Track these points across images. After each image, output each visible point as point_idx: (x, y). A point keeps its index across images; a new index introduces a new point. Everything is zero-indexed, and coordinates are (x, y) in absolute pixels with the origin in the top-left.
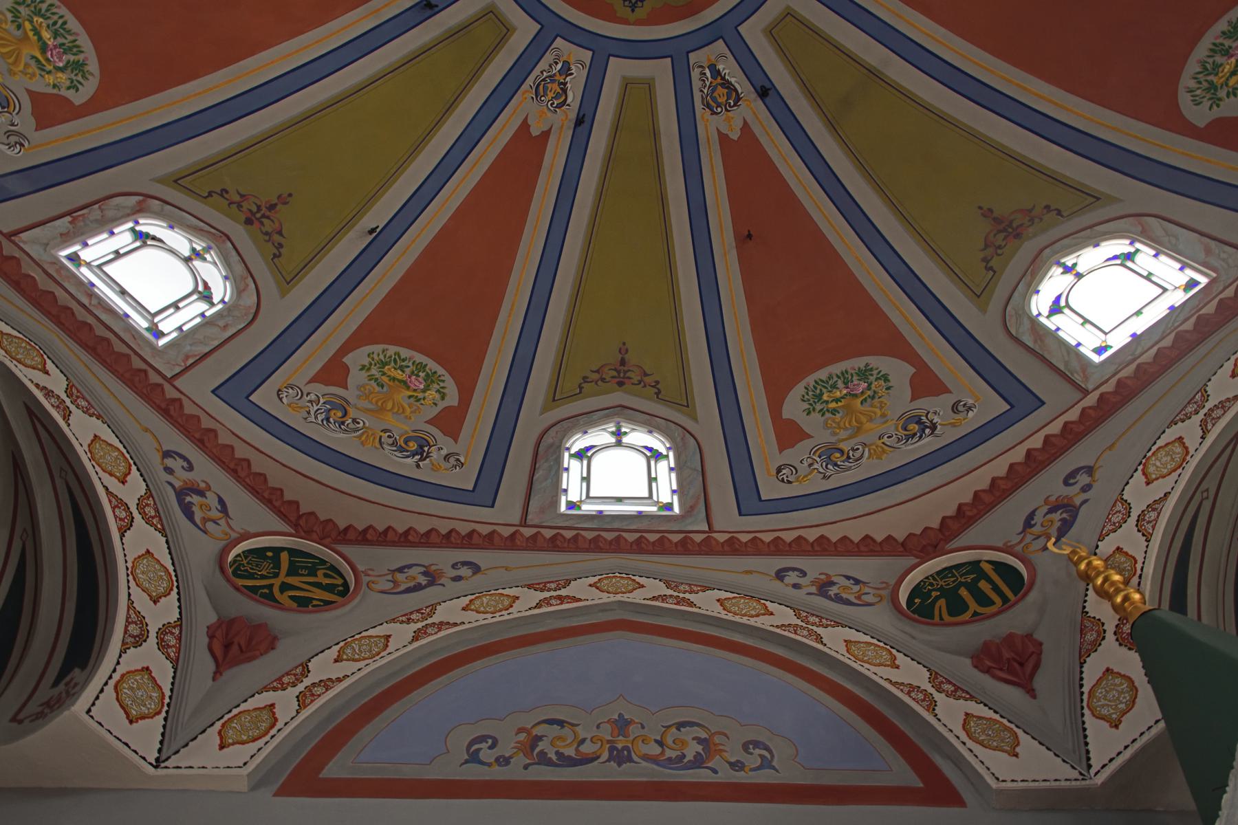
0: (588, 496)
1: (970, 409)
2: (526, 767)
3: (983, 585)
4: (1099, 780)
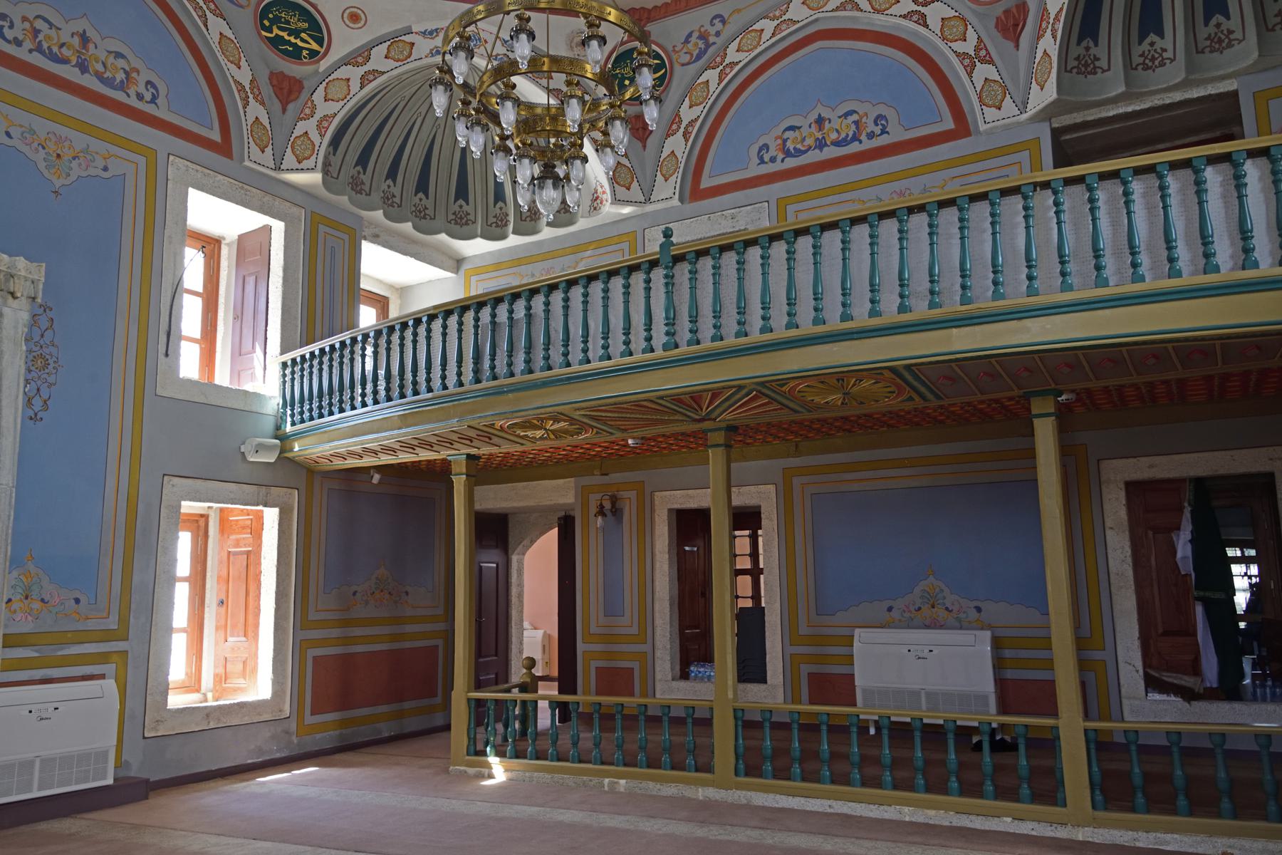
2: (31, 51)
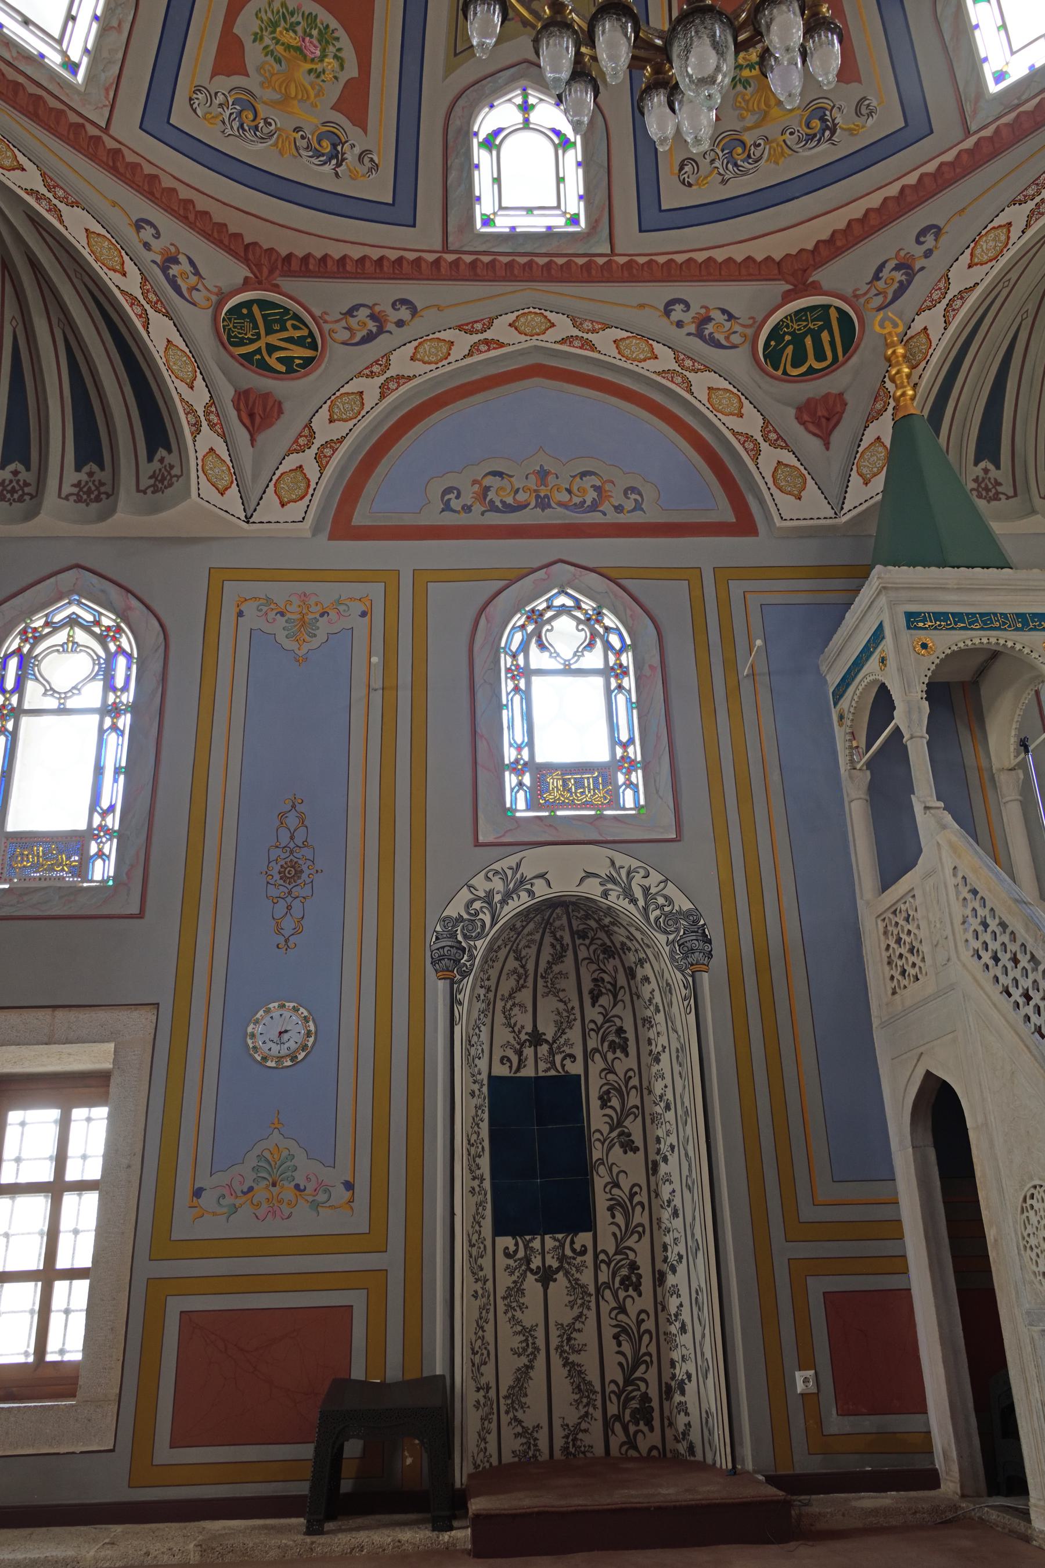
0: (501, 208)
1: (870, 114)
2: (483, 514)
3: (825, 336)
4: (844, 519)
